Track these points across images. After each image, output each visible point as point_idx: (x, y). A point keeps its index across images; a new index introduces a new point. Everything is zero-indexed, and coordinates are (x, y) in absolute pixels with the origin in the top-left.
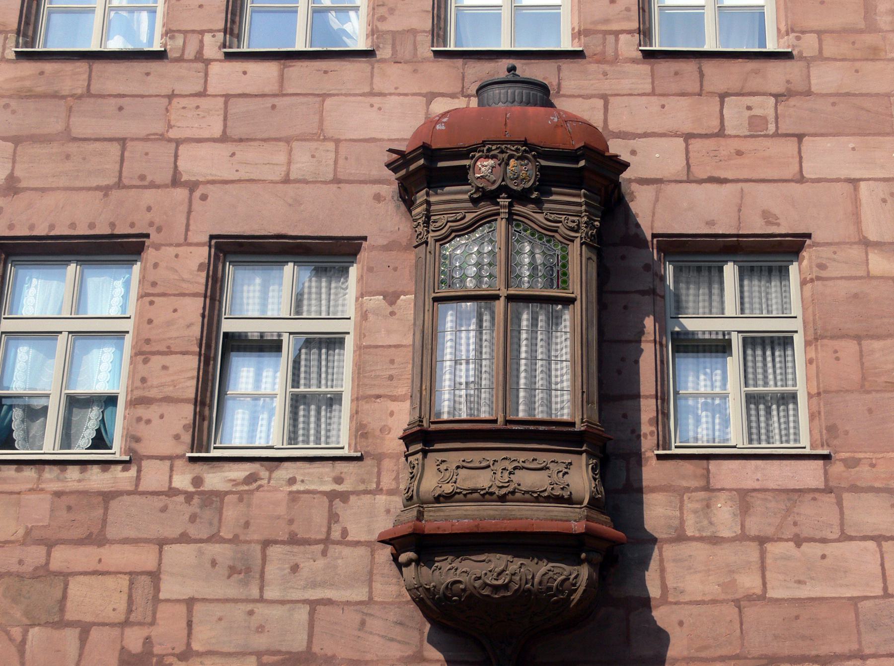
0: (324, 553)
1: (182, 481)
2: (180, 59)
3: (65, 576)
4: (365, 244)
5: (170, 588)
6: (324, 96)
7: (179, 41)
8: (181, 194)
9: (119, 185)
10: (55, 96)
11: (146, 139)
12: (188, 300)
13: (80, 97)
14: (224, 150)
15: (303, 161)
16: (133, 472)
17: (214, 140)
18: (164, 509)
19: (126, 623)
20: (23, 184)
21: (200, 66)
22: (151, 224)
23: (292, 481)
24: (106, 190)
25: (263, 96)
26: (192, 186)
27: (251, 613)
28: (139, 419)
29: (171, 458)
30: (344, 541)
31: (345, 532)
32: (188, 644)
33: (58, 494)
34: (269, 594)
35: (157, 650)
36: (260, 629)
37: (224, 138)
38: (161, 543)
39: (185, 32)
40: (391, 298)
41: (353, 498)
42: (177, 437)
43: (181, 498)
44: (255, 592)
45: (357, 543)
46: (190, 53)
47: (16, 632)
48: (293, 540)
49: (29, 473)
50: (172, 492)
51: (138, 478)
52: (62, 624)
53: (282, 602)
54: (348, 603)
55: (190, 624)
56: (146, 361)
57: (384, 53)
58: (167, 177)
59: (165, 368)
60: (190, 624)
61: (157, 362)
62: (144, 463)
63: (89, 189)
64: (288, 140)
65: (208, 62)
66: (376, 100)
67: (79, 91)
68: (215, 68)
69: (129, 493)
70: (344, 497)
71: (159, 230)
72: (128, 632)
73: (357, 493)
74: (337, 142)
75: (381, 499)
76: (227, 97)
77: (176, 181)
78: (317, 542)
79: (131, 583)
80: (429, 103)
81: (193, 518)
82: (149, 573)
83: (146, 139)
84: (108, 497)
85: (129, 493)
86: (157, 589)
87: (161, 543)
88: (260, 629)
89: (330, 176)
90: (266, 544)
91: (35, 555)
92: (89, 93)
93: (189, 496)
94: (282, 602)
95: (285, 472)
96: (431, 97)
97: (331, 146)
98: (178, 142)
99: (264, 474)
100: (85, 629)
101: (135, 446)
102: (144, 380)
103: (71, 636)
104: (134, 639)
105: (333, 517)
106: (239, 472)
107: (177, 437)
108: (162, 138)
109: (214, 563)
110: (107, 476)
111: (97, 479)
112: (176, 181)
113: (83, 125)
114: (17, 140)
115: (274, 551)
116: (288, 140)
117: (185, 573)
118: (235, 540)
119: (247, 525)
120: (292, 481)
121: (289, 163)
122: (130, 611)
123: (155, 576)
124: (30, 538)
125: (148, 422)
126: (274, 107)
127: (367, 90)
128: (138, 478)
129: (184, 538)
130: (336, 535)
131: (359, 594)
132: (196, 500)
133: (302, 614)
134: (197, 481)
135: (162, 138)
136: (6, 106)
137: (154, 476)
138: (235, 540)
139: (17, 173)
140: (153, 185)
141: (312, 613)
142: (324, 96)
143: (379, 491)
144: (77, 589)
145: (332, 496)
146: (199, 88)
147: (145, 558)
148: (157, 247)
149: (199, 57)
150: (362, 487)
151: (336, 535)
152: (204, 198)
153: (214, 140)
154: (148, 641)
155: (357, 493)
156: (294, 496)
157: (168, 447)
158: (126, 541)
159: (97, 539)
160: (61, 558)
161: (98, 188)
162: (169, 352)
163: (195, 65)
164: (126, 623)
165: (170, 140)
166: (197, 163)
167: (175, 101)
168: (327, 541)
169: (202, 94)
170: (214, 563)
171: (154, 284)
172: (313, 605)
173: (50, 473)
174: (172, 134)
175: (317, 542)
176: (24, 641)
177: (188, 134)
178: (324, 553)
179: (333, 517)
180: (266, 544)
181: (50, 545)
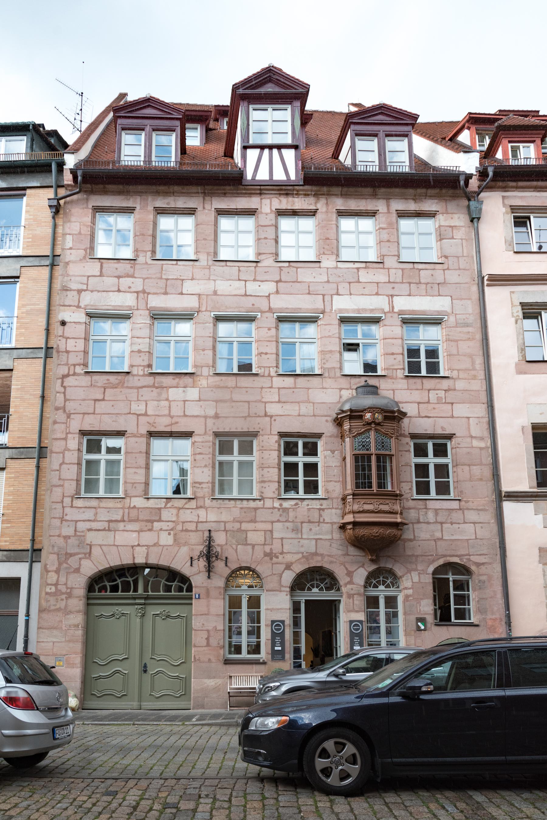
0: (319, 525)
1: (277, 504)
2: (263, 376)
3: (246, 531)
4: (324, 435)
5: (276, 535)
6: (309, 389)
7: (263, 370)
8: (268, 419)
9: (249, 416)
10: (226, 387)
11: (255, 402)
12: (273, 452)
13: (234, 388)
14: (280, 405)
15: (303, 410)
16: (262, 502)
17: (276, 402)
18: (272, 513)
19: (264, 544)
20: (220, 416)
21: (270, 378)
22: (260, 428)
23: (308, 505)
24: (245, 417)
25: (290, 388)
26: (271, 417)
27: (299, 542)
28: (262, 487)
29: (273, 498)
30: (324, 522)
31: (324, 520)
32: (283, 550)
33: (241, 508)
34: (304, 537)
35: (274, 552)
36: (302, 546)
37: (279, 402)
38: (272, 522)
39: (264, 367)
40: (333, 452)
41: (326, 510)
42: (274, 492)
43: (277, 510)
44: (300, 536)
45: (328, 523)
46: (266, 374)
47: (234, 546)
48: (310, 522)
49: (232, 502)
50: (274, 508)
51: (264, 504)
52: (247, 544)
53: (308, 539)
54: (326, 539)
55: (282, 545)
56: (263, 470)
57: (326, 375)
58: (263, 414)
59: (268, 472)
60: (282, 545)
61: (266, 470)
62: (265, 500)
63: (240, 417)
64: (298, 403)
65: (272, 377)
66: (324, 390)
67: (234, 386)
68: (274, 379)
69: (262, 508)
70: (323, 510)
71: (262, 430)
72: (265, 546)
73: (327, 509)
74: (313, 403)
75: (334, 510)
76: (279, 388)
77: (266, 415)
78: (316, 522)
79: (265, 533)
80: (340, 391)
81: (281, 515)
82: (270, 531)
83: (255, 402)
84: (256, 509)
85: (262, 508)
86: (272, 535)
87: (272, 522)
88: (302, 546)
89: (312, 414)
90: (302, 523)
91: (237, 526)
92: (236, 387)
93: (279, 509)
94: (308, 539)
95: (306, 503)
96: (341, 389)
97: (312, 404)
98: (265, 403)
99: (300, 503)
100: (253, 546)
101: (262, 495)
102: (262, 475)
103: (250, 547)
104: (267, 549)
105: (320, 516)
106: (293, 502)
107: (274, 492)
108: (260, 401)
109: (288, 528)
110: (255, 503)
111: (252, 504)
112: (266, 415)
113: (236, 397)
114: (217, 401)
115: (304, 525)
116: (298, 403)
117: (279, 531)
118: (293, 522)
119: (296, 517)
120: (308, 505)
121: (300, 410)
122: (265, 541)
123: (271, 531)
124: (235, 521)
125: (265, 488)
126: (293, 392)
127: (321, 387)
128: (264, 504)
129: (278, 521)
130: (322, 520)
131: (329, 537)
132: (281, 510)
133: (314, 542)
134: (281, 505)
135: (260, 401)
136: (212, 390)
137: (268, 503)
138: (293, 522)
139: (218, 412)
140: (259, 416)
141: (316, 542)
142: (309, 389)
143: (333, 508)
144: (250, 534)
145: (320, 509)
146: (270, 386)
147: (268, 527)
148: (262, 435)
149: (269, 375)
150: (328, 507)
151: (322, 520)
152: (275, 420)
153: (276, 402)
154: (271, 549)
155: (327, 509)
156: (309, 509)
157: (272, 495)
158: (262, 522)
159: (254, 521)
160: (245, 526)
161: (243, 417)
162: (269, 467)
163: (268, 378)
164: (264, 544)
165: (263, 402)
166: (273, 409)
167: (263, 389)
168: (319, 522)
169: (271, 387)
170: (288, 528)
171: (263, 447)
172: (316, 540)
173: (238, 502)
174: (263, 400)
175: (316, 522)
176: (237, 549)
177: (268, 400)
178: (319, 525)
179: (320, 516)
180: (302, 523)
181: (241, 522)
